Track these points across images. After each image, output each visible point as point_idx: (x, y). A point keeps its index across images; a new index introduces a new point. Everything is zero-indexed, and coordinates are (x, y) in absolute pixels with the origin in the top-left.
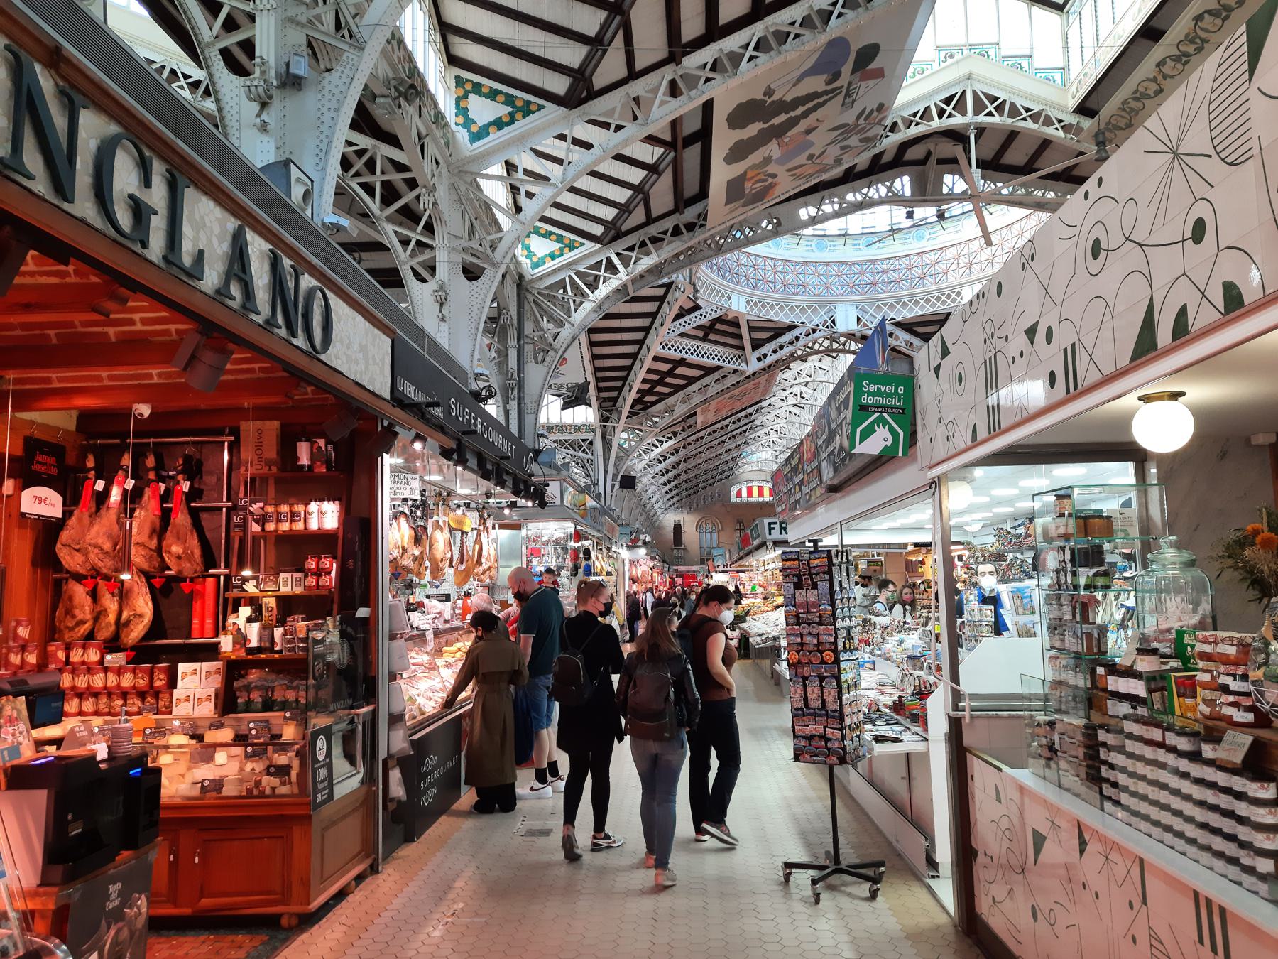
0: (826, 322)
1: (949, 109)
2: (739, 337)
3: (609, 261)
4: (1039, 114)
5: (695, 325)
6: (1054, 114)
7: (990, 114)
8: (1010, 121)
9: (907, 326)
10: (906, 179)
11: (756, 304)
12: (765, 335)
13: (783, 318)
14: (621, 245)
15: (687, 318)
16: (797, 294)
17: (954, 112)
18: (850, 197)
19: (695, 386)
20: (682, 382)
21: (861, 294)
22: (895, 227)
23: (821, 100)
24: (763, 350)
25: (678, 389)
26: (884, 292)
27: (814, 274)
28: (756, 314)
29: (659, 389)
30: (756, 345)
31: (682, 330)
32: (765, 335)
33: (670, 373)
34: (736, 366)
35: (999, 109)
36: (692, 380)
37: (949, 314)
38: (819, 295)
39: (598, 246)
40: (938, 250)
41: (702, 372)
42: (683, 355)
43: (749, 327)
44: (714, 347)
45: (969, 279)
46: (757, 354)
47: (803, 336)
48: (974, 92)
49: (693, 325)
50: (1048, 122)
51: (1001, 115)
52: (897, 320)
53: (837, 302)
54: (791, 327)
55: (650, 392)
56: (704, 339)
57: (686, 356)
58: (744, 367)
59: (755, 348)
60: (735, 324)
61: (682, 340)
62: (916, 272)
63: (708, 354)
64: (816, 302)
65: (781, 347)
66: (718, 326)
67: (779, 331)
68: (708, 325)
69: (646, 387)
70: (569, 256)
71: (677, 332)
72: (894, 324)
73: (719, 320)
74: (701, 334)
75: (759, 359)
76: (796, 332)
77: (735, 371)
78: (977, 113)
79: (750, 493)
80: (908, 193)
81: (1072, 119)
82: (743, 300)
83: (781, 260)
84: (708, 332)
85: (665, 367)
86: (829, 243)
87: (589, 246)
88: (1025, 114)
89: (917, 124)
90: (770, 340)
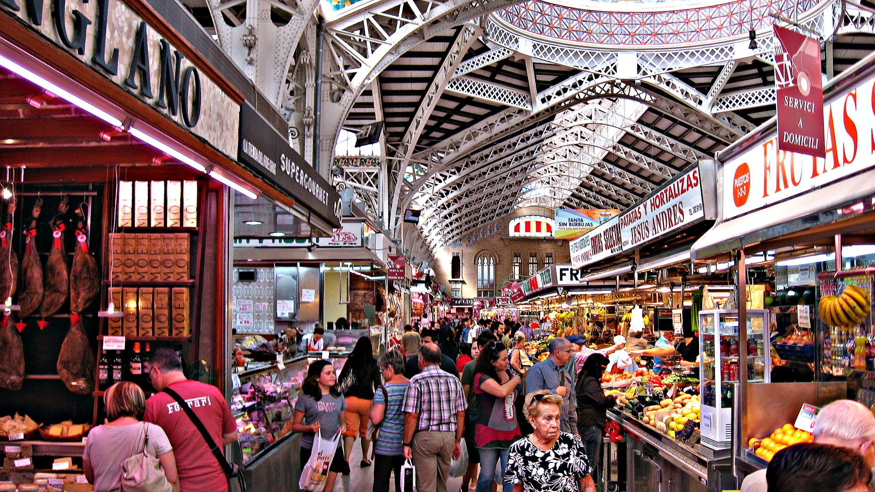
0: (608, 68)
2: (525, 79)
5: (483, 65)
9: (684, 76)
11: (542, 48)
13: (567, 63)
15: (475, 59)
25: (463, 126)
27: (597, 22)
29: (446, 126)
31: (470, 70)
33: (457, 111)
34: (521, 107)
36: (477, 118)
37: (721, 67)
38: (602, 43)
42: (470, 94)
43: (535, 70)
45: (737, 37)
46: (541, 96)
47: (586, 80)
49: (481, 66)
52: (674, 70)
55: (436, 128)
56: (492, 79)
57: (473, 95)
58: (529, 108)
60: (521, 65)
62: (693, 26)
65: (565, 90)
66: (505, 68)
68: (495, 66)
69: (433, 123)
71: (465, 72)
72: (671, 73)
73: (506, 62)
74: (488, 74)
75: (543, 101)
76: (579, 77)
82: (530, 44)
83: (567, 8)
84: (493, 73)
85: (452, 105)
90: (554, 83)
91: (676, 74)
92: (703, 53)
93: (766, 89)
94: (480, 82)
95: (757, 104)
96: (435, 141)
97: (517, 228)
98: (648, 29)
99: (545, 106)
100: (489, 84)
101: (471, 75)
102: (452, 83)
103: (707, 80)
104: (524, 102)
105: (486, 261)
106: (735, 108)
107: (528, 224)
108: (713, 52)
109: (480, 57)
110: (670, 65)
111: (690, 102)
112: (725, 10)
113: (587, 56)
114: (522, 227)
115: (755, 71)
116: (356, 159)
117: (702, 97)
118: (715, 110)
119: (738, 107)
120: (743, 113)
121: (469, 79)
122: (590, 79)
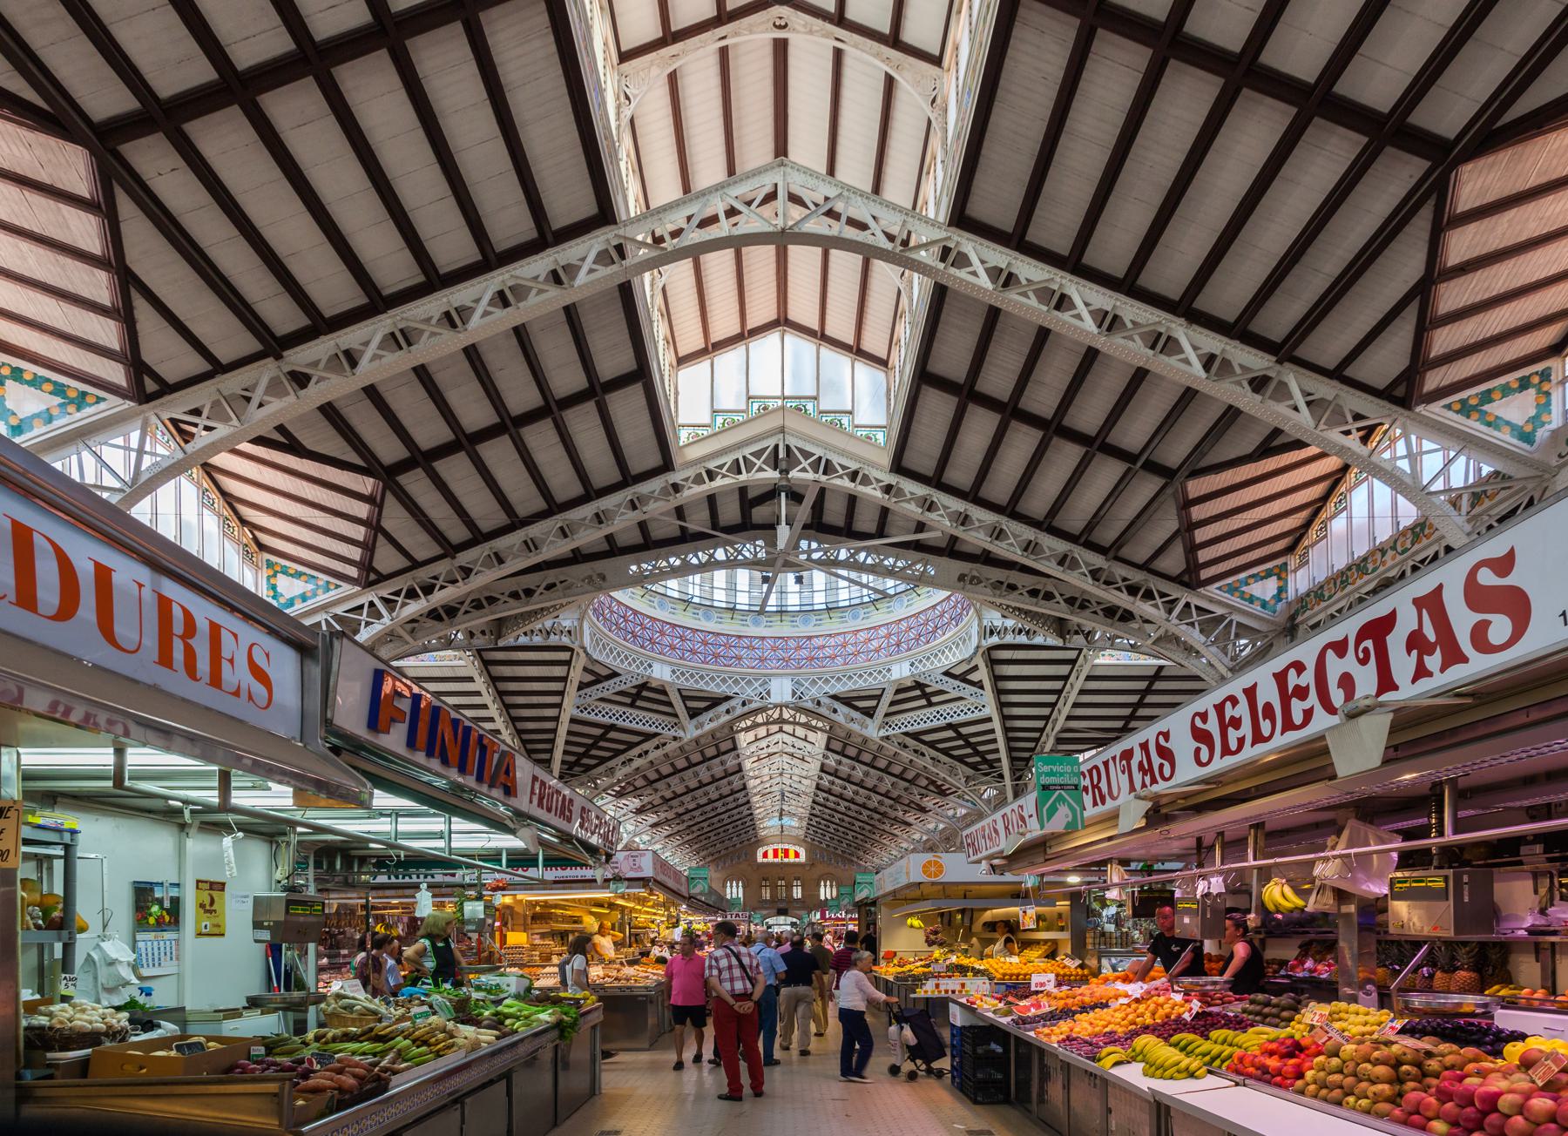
1: (759, 463)
3: (372, 604)
6: (874, 474)
7: (804, 470)
8: (824, 478)
9: (847, 701)
10: (760, 542)
13: (715, 689)
15: (606, 684)
17: (765, 467)
20: (622, 747)
24: (701, 718)
25: (617, 753)
29: (594, 752)
30: (694, 714)
31: (600, 695)
33: (603, 737)
34: (673, 733)
35: (815, 466)
36: (631, 746)
41: (640, 738)
46: (694, 721)
48: (788, 448)
50: (866, 481)
51: (816, 472)
54: (728, 698)
56: (632, 705)
58: (681, 734)
61: (603, 705)
62: (850, 649)
63: (638, 720)
64: (750, 674)
66: (645, 693)
67: (715, 702)
68: (634, 691)
70: (323, 598)
73: (644, 686)
74: (628, 700)
76: (732, 703)
77: (675, 738)
80: (759, 555)
81: (892, 479)
87: (347, 589)
88: (841, 472)
89: (724, 476)
90: (707, 709)
91: (835, 697)
92: (861, 676)
93: (931, 709)
95: (929, 725)
96: (589, 768)
97: (765, 855)
98: (804, 653)
99: (699, 732)
101: (602, 700)
103: (873, 703)
106: (905, 730)
108: (871, 674)
109: (612, 682)
110: (827, 689)
111: (855, 727)
112: (883, 632)
113: (736, 682)
114: (771, 854)
115: (918, 693)
117: (868, 720)
118: (882, 733)
119: (910, 729)
120: (915, 736)
121: (598, 703)
122: (744, 704)
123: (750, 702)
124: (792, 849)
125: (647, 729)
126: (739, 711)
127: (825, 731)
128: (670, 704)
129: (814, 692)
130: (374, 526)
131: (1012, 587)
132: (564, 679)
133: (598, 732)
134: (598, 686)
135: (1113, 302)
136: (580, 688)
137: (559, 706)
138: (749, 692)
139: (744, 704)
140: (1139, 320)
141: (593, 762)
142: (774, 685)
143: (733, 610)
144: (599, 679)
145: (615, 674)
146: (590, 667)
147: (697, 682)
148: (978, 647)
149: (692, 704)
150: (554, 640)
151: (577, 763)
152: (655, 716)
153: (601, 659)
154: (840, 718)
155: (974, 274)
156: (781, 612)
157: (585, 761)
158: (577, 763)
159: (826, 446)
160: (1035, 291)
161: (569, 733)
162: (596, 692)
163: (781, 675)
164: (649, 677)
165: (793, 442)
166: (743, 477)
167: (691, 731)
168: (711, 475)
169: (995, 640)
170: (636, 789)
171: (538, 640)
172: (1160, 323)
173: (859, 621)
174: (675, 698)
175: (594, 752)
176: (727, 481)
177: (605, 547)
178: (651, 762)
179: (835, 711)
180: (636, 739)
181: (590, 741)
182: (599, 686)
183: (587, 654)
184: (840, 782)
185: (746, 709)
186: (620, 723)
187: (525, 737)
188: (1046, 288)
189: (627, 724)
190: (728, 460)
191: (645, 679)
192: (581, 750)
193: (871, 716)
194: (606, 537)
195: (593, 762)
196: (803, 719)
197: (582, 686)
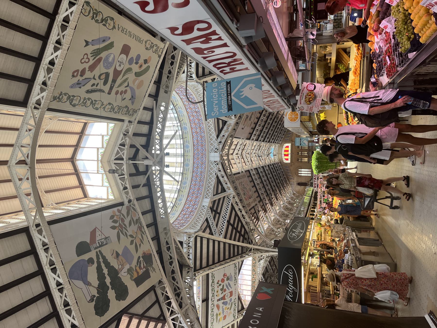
4: (124, 135)
5: (213, 221)
6: (124, 128)
7: (123, 154)
9: (220, 131)
12: (220, 187)
14: (167, 314)
15: (211, 224)
16: (204, 176)
18: (159, 194)
19: (239, 213)
20: (237, 218)
21: (206, 151)
22: (181, 138)
23: (101, 260)
25: (239, 220)
26: (205, 142)
28: (211, 195)
29: (239, 229)
30: (223, 190)
31: (215, 226)
32: (220, 187)
33: (233, 226)
35: (122, 150)
36: (236, 214)
38: (205, 167)
39: (166, 324)
40: (190, 123)
41: (233, 211)
42: (226, 222)
44: (223, 209)
47: (221, 173)
48: (116, 159)
49: (213, 221)
51: (124, 149)
53: (208, 160)
54: (217, 177)
56: (220, 214)
57: (226, 221)
58: (232, 195)
59: (225, 191)
62: (198, 130)
63: (226, 212)
64: (208, 168)
66: (215, 209)
67: (219, 182)
68: (214, 213)
73: (212, 209)
74: (217, 215)
76: (219, 175)
78: (122, 159)
79: (287, 155)
83: (191, 182)
86: (186, 162)
89: (126, 183)
91: (218, 136)
92: (209, 126)
94: (220, 219)
96: (246, 231)
97: (287, 159)
98: (200, 148)
99: (231, 189)
100: (222, 214)
101: (217, 226)
102: (220, 234)
103: (220, 122)
104: (229, 197)
105: (300, 172)
107: (285, 155)
109: (210, 221)
110: (214, 139)
111: (230, 128)
113: (211, 174)
114: (286, 157)
116: (253, 262)
117: (228, 123)
121: (218, 227)
122: (220, 171)
123: (219, 168)
124: (284, 149)
125: (229, 209)
126: (223, 173)
127: (232, 139)
128: (219, 199)
129: (216, 145)
130: (141, 317)
131: (170, 72)
132: (208, 240)
133: (230, 227)
134: (212, 228)
135: (51, 44)
136: (212, 234)
137: (219, 242)
138: (215, 169)
139: (220, 171)
140: (57, 34)
141: (243, 230)
142: (212, 159)
143: (182, 173)
144: (208, 226)
145: (207, 220)
146: (202, 231)
147: (210, 189)
148: (197, 82)
149: (220, 191)
150: (192, 244)
151: (244, 236)
152: (224, 205)
153: (200, 226)
154: (226, 134)
155: (43, 97)
156: (184, 156)
157: (243, 233)
158: (244, 236)
159: (115, 146)
160: (48, 74)
161: (230, 239)
162: (213, 228)
163: (208, 156)
164: (208, 207)
165: (113, 158)
166: (126, 177)
167: (231, 192)
168: (125, 188)
169: (194, 76)
170: (255, 212)
171: (192, 251)
172: (58, 25)
173: (187, 127)
174: (217, 197)
175: (239, 229)
176: (127, 183)
177: (153, 227)
178: (243, 207)
179: (224, 136)
180: (234, 213)
181: (234, 231)
182: (211, 226)
183: (198, 232)
184: (255, 132)
185: (222, 170)
186: (227, 219)
187: (232, 255)
188: (47, 70)
189: (227, 216)
190: (119, 181)
191: (209, 208)
192: (238, 234)
193: (226, 122)
194: (147, 228)
195: (243, 230)
196: (227, 147)
197: (211, 233)
